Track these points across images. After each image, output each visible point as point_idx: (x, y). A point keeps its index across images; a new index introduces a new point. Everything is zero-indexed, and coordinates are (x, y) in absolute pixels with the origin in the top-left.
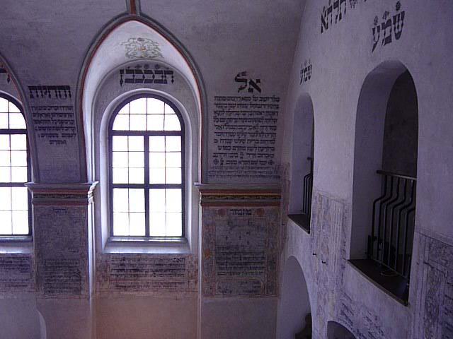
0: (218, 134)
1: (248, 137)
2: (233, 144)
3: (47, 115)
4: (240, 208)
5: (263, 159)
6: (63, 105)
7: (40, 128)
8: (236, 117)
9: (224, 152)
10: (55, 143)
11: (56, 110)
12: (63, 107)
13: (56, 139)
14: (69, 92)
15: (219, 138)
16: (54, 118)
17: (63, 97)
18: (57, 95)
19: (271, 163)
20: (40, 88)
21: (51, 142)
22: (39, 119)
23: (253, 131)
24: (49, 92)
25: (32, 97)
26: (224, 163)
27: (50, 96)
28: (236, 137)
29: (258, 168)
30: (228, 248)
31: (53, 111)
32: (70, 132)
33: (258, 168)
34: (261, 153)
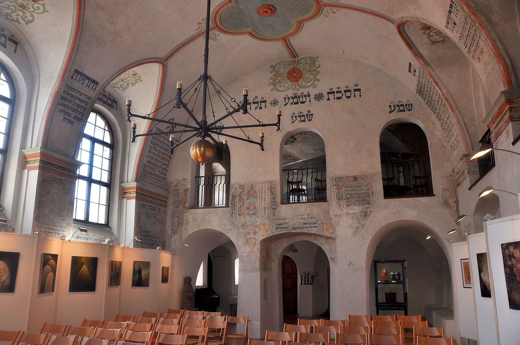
0: (150, 152)
1: (160, 160)
2: (153, 161)
3: (72, 96)
4: (151, 205)
5: (162, 176)
6: (86, 94)
7: (64, 105)
8: (159, 144)
9: (149, 165)
10: (67, 120)
11: (81, 95)
12: (85, 95)
13: (68, 118)
14: (96, 87)
15: (149, 155)
16: (76, 101)
17: (90, 88)
18: (87, 85)
19: (165, 179)
20: (81, 74)
21: (64, 119)
22: (66, 97)
23: (163, 156)
24: (85, 80)
25: (72, 78)
26: (147, 172)
27: (83, 83)
28: (155, 157)
29: (160, 181)
30: (145, 232)
31: (78, 95)
32: (80, 116)
33: (160, 181)
34: (162, 171)
